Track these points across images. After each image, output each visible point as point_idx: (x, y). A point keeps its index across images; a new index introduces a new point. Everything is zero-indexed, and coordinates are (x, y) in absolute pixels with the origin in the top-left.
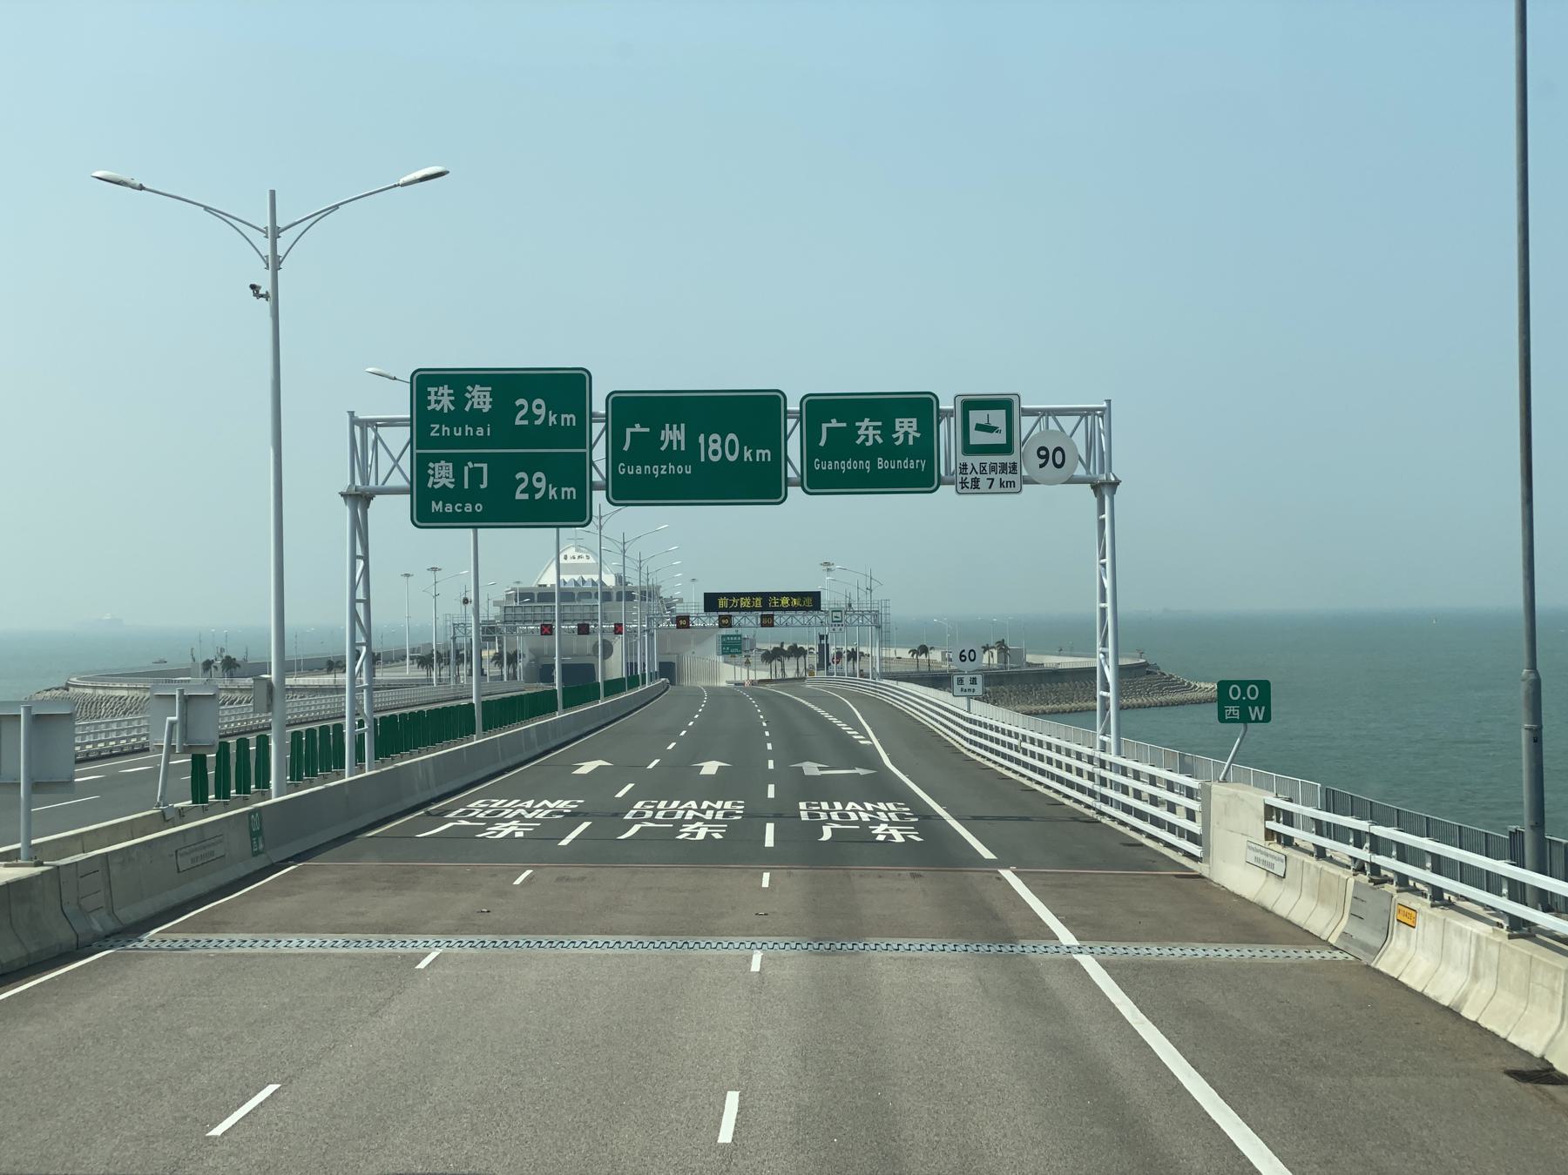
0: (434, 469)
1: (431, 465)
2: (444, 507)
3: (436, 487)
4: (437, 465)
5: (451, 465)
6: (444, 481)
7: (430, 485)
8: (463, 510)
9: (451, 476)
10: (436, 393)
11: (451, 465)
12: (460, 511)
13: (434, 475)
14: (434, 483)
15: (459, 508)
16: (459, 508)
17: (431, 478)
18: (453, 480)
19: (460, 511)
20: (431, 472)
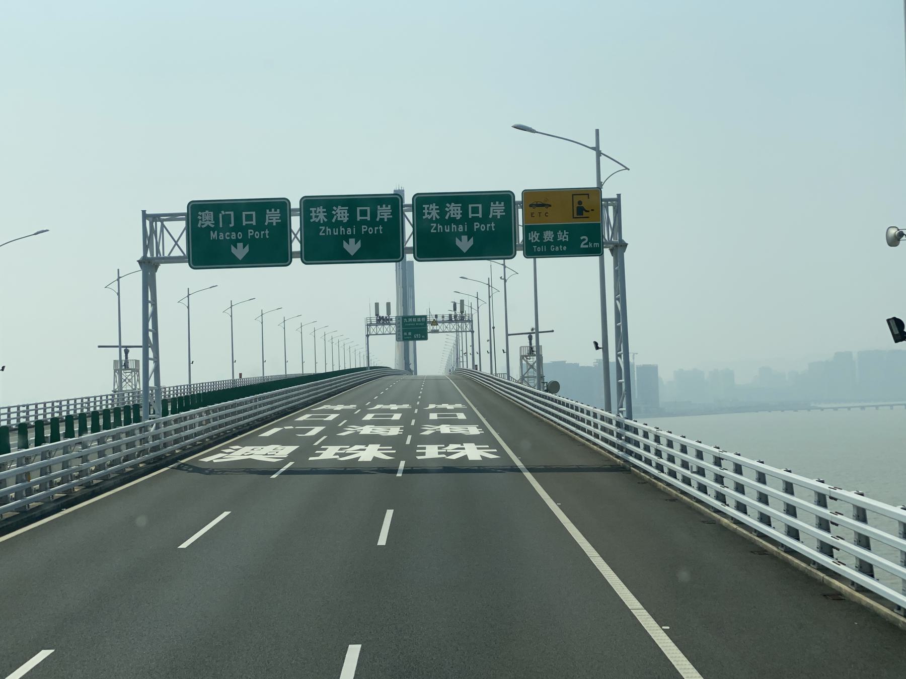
0: (201, 216)
1: (200, 213)
2: (218, 235)
3: (203, 226)
4: (203, 213)
5: (212, 213)
6: (209, 223)
7: (199, 226)
8: (230, 237)
9: (212, 220)
10: (315, 212)
11: (212, 213)
12: (228, 238)
13: (201, 220)
14: (202, 224)
15: (228, 236)
16: (228, 236)
17: (200, 221)
18: (214, 222)
19: (228, 238)
20: (199, 217)
